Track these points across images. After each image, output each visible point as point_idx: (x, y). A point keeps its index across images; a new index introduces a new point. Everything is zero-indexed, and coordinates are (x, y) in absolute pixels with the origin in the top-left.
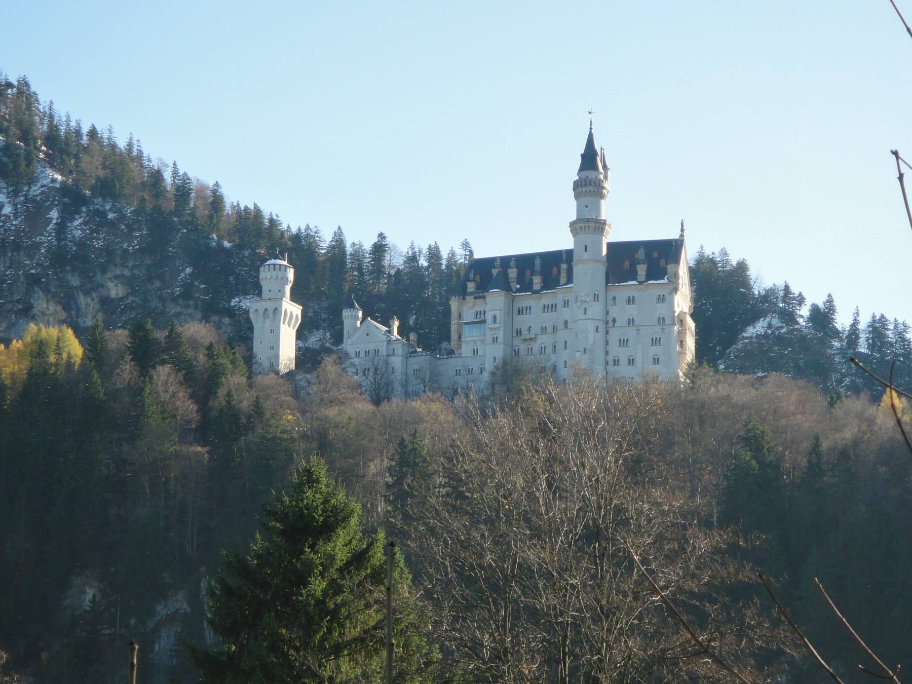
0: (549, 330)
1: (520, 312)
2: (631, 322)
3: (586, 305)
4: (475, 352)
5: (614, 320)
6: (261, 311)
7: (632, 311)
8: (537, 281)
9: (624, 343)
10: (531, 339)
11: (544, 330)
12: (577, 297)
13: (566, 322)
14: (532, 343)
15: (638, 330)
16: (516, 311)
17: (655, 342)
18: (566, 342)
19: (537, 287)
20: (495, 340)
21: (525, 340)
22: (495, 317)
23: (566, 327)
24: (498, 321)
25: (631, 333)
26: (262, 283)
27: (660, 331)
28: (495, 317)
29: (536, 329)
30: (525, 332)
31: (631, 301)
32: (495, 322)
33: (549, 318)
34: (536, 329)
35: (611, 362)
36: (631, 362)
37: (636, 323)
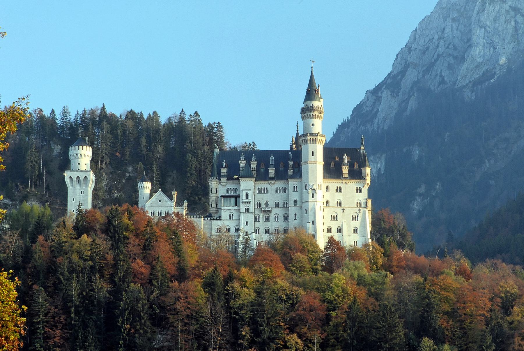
0: (281, 205)
1: (260, 191)
2: (339, 204)
3: (313, 192)
4: (231, 217)
5: (327, 202)
6: (74, 179)
7: (339, 196)
8: (272, 171)
9: (334, 218)
10: (269, 211)
11: (277, 205)
12: (306, 186)
13: (295, 201)
14: (269, 213)
15: (343, 210)
16: (256, 191)
17: (355, 218)
18: (295, 215)
19: (272, 175)
20: (247, 210)
21: (265, 211)
22: (247, 195)
23: (295, 205)
24: (250, 197)
25: (339, 210)
26: (70, 158)
27: (358, 212)
28: (247, 195)
29: (271, 204)
30: (263, 205)
31: (339, 190)
32: (247, 198)
33: (280, 197)
34: (271, 204)
35: (326, 230)
36: (339, 230)
37: (342, 205)
